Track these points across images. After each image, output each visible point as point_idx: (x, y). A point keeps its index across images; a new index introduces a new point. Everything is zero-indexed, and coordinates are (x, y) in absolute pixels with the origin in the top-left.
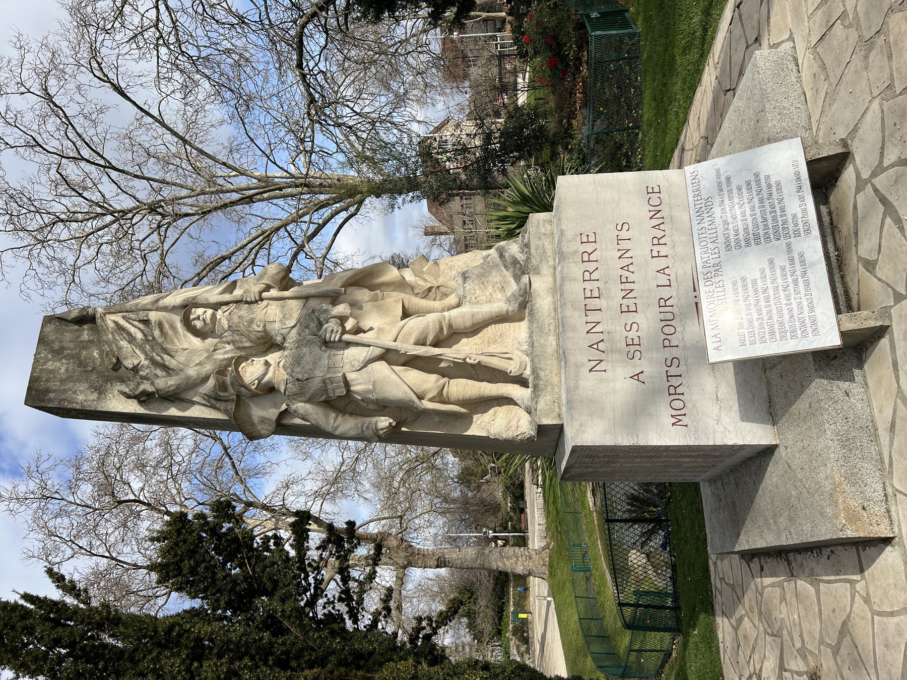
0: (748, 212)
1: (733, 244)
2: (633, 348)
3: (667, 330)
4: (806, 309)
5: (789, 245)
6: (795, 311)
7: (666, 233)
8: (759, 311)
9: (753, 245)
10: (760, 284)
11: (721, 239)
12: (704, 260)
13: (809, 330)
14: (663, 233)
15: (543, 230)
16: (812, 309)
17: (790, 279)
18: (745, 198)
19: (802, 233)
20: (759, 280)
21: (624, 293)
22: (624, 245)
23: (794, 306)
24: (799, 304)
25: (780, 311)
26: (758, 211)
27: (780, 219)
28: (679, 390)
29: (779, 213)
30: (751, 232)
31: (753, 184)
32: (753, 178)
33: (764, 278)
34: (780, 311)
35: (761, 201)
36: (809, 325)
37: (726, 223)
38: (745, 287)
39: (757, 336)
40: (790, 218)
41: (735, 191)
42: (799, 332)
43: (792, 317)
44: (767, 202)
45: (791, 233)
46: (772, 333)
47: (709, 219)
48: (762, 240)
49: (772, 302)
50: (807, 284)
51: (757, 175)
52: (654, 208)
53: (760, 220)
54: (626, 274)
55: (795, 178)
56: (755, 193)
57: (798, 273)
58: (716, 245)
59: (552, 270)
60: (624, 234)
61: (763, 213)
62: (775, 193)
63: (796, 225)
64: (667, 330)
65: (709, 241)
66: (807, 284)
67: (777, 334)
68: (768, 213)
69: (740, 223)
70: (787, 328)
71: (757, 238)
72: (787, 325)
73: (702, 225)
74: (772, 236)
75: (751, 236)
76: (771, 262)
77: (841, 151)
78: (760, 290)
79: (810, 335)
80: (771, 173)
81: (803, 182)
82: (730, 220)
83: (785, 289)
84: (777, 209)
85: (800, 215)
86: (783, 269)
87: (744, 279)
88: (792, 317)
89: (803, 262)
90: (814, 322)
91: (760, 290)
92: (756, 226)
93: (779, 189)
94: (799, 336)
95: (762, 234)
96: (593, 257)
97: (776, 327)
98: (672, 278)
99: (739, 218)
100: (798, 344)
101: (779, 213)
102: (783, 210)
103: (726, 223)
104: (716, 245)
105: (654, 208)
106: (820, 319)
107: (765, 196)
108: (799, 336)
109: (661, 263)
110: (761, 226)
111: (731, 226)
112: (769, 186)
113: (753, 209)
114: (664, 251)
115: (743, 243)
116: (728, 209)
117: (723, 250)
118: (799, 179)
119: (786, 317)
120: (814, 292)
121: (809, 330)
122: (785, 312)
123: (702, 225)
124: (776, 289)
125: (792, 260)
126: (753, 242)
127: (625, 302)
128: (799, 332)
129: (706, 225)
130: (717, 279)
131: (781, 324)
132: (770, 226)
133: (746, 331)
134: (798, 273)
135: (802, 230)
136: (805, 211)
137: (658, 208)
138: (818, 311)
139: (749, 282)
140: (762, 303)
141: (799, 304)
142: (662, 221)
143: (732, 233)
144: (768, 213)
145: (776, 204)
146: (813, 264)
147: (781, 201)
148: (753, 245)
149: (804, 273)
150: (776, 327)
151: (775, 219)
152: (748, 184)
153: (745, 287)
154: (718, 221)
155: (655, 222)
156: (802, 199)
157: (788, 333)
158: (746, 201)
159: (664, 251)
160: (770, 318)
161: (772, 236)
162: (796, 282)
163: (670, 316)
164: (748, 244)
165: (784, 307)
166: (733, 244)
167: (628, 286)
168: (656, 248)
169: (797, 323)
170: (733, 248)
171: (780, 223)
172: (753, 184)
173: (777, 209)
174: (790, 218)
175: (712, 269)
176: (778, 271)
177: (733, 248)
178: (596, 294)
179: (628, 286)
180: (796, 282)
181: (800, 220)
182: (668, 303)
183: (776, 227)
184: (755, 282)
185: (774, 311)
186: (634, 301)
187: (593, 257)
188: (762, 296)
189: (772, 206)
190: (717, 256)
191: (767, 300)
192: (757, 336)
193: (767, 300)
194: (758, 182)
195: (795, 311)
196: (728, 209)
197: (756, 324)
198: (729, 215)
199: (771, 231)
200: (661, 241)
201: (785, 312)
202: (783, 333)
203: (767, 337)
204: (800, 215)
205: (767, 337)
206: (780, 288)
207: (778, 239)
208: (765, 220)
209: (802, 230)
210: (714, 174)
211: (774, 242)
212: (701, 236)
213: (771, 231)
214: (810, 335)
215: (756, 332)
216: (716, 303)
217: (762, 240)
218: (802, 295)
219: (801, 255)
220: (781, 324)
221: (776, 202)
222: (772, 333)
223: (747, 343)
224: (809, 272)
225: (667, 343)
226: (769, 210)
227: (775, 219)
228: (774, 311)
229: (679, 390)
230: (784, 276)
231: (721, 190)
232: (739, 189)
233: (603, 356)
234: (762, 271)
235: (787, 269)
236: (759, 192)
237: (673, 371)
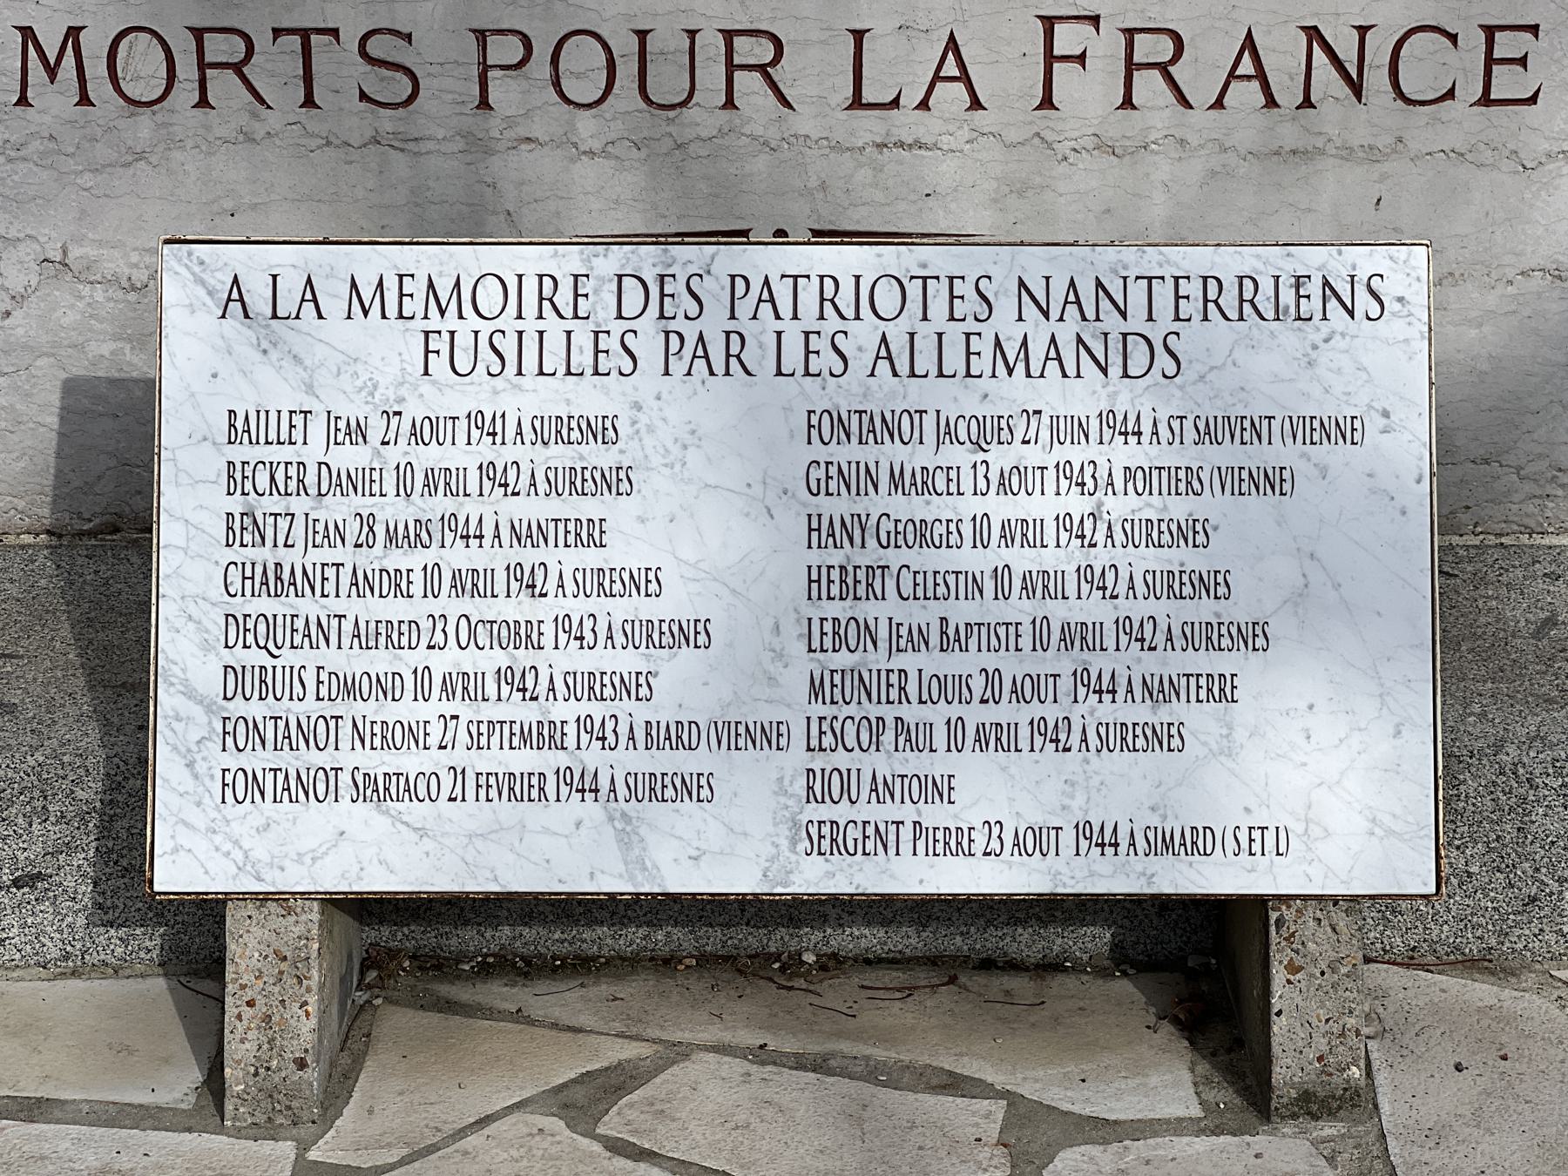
0: (1022, 560)
1: (846, 453)
5: (769, 736)
7: (1201, 118)
8: (415, 536)
9: (815, 557)
11: (887, 393)
12: (782, 292)
13: (258, 760)
14: (1202, 91)
16: (371, 789)
17: (565, 711)
18: (1121, 556)
19: (825, 812)
20: (591, 558)
23: (407, 710)
24: (414, 735)
25: (390, 635)
26: (1020, 609)
27: (938, 714)
29: (975, 715)
30: (894, 558)
31: (1203, 610)
32: (1238, 611)
33: (602, 582)
34: (390, 635)
35: (1078, 636)
36: (285, 759)
37: (988, 432)
38: (575, 482)
39: (272, 503)
40: (937, 764)
41: (1180, 508)
42: (256, 710)
43: (350, 689)
44: (1064, 664)
45: (841, 759)
46: (276, 581)
47: (1038, 350)
48: (835, 609)
49: (453, 606)
50: (519, 788)
51: (1252, 636)
52: (1379, 49)
53: (962, 612)
55: (1173, 825)
56: (1139, 609)
57: (593, 757)
58: (860, 363)
61: (1003, 636)
62: (1108, 711)
63: (882, 789)
65: (897, 333)
66: (519, 788)
67: (266, 605)
68: (990, 661)
69: (970, 506)
70: (288, 657)
72: (306, 658)
73: (1006, 307)
74: (843, 659)
75: (871, 555)
76: (689, 634)
77: (1279, 1074)
78: (529, 556)
79: (232, 761)
80: (1244, 710)
81: (1138, 863)
82: (1000, 458)
83: (517, 683)
84: (1004, 712)
85: (935, 815)
86: (635, 687)
87: (615, 482)
88: (350, 689)
89: (653, 788)
90: (301, 787)
91: (529, 556)
92: (928, 587)
93: (1124, 738)
94: (238, 707)
95: (869, 610)
97: (309, 607)
99: (1001, 508)
100: (190, 694)
101: (975, 715)
102: (994, 738)
103: (988, 432)
104: (860, 363)
105: (1379, 49)
106: (313, 823)
107: (1100, 663)
108: (238, 707)
109: (1007, 71)
110: (924, 614)
111: (959, 456)
112: (1160, 691)
113: (1040, 585)
114: (1087, 93)
115: (839, 506)
116: (1077, 454)
117: (820, 395)
118: (1164, 844)
120: (472, 814)
121: (258, 760)
122: (380, 662)
123: (1006, 307)
124: (523, 635)
125: (677, 736)
126: (835, 557)
128: (256, 710)
129: (1004, 323)
130: (648, 344)
132: (908, 661)
133: (313, 452)
134: (593, 757)
135: (842, 812)
136: (956, 843)
137: (1376, 80)
139: (588, 508)
140: (458, 557)
141: (414, 735)
142: (1288, 96)
143: (919, 457)
144: (990, 661)
145: (1036, 710)
146: (627, 837)
147: (1053, 736)
148: (815, 557)
149: (587, 787)
150: (309, 607)
151: (946, 688)
152: (1211, 585)
153: (575, 482)
154: (1013, 393)
155: (1284, 57)
156: (1036, 841)
157: (257, 657)
158: (1101, 558)
159: (1087, 93)
160: (362, 584)
161: (843, 659)
162: (548, 736)
164: (818, 531)
165: (420, 657)
166: (846, 453)
168: (1105, 48)
169: (310, 707)
170: (819, 452)
171: (912, 713)
172: (1203, 610)
173: (1004, 712)
174: (937, 764)
175: (714, 324)
176: (626, 661)
177: (819, 452)
180: (548, 736)
181: (907, 813)
183: (896, 686)
184: (590, 534)
185: (394, 609)
188: (491, 558)
189: (1027, 689)
190: (793, 357)
191: (468, 584)
192: (272, 503)
193: (468, 584)
194: (1208, 637)
195: (371, 710)
196: (1077, 454)
197: (338, 509)
198: (1032, 456)
199: (878, 659)
201: (380, 662)
202: (269, 634)
203: (265, 554)
204: (935, 815)
205: (265, 554)
206: (524, 657)
207: (816, 690)
208: (952, 639)
209: (842, 812)
210: (1328, 409)
211: (799, 669)
212: (939, 291)
213: (878, 659)
214: (232, 761)
215: (299, 505)
216: (508, 322)
217: (835, 609)
218: (460, 756)
219: (692, 788)
221: (1052, 713)
222: (276, 581)
223: (239, 453)
224: (590, 810)
226: (1011, 666)
227: (946, 688)
228: (394, 609)
230: (591, 686)
231: (1207, 433)
232: (1190, 533)
234: (644, 582)
235: (625, 706)
236: (1135, 633)
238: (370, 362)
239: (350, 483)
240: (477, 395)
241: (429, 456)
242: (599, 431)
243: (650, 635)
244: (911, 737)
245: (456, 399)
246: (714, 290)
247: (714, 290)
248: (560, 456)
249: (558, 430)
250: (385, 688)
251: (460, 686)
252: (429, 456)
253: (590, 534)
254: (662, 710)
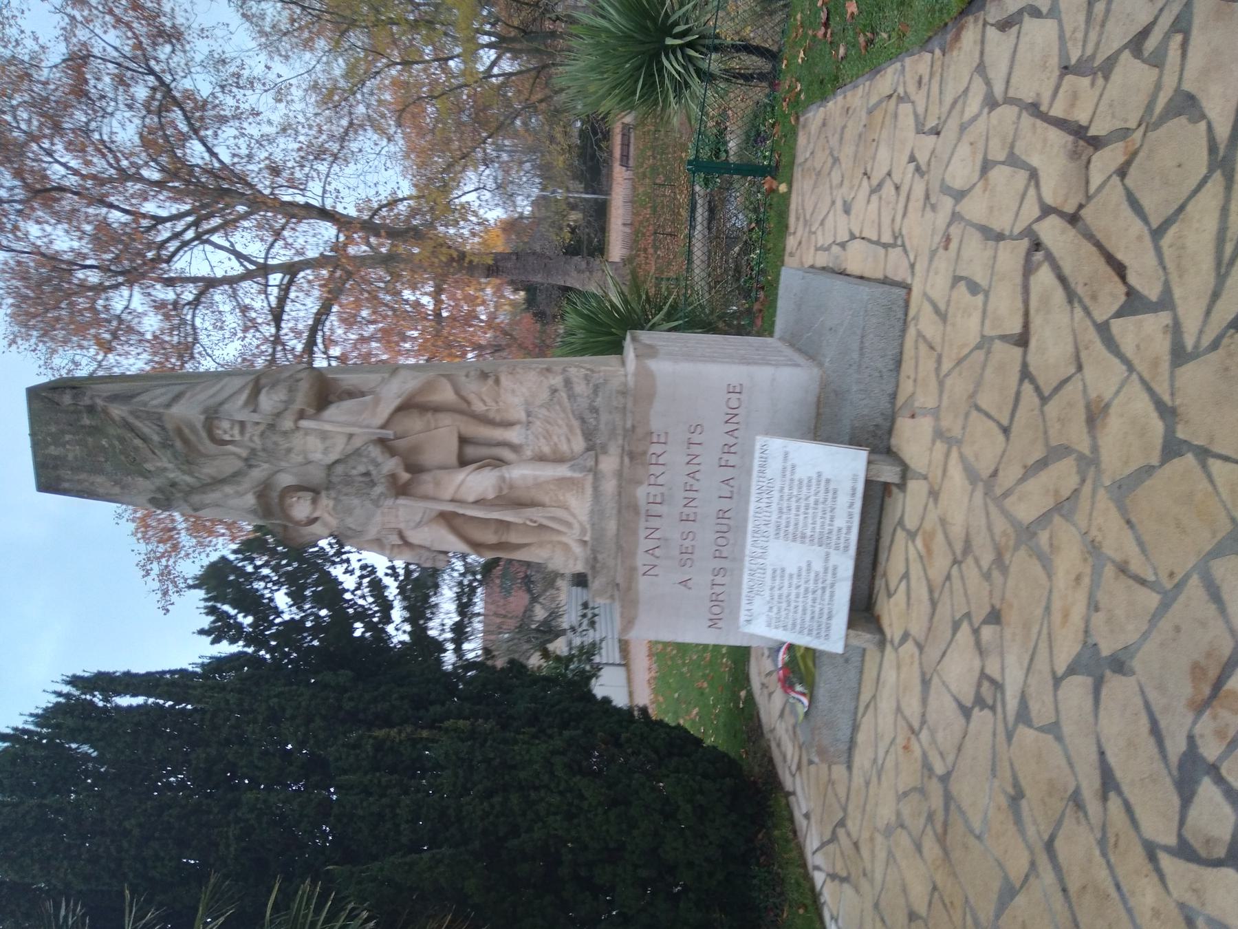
2: (686, 556)
3: (721, 541)
4: (825, 616)
5: (828, 555)
6: (817, 615)
10: (795, 581)
13: (823, 634)
15: (615, 404)
16: (830, 618)
21: (686, 501)
22: (695, 449)
27: (827, 528)
28: (720, 597)
29: (828, 522)
33: (799, 576)
34: (804, 610)
38: (782, 576)
44: (820, 506)
46: (794, 625)
54: (691, 481)
59: (619, 450)
60: (696, 438)
63: (839, 538)
64: (721, 541)
69: (792, 516)
71: (803, 537)
83: (814, 592)
87: (783, 570)
89: (834, 574)
90: (828, 628)
96: (661, 460)
98: (735, 490)
102: (832, 519)
109: (729, 473)
110: (810, 526)
115: (790, 536)
117: (772, 536)
119: (808, 617)
121: (823, 634)
124: (806, 590)
125: (826, 570)
127: (686, 510)
130: (761, 561)
131: (803, 621)
132: (818, 530)
138: (834, 622)
140: (793, 597)
149: (832, 585)
150: (799, 621)
162: (824, 589)
163: (724, 528)
164: (794, 540)
167: (691, 494)
168: (726, 457)
174: (835, 530)
178: (658, 500)
179: (691, 494)
180: (824, 589)
182: (727, 515)
185: (800, 609)
186: (694, 510)
187: (661, 460)
188: (794, 592)
193: (797, 596)
195: (817, 615)
197: (783, 613)
200: (733, 450)
202: (802, 628)
204: (844, 531)
205: (790, 626)
211: (816, 547)
219: (835, 568)
220: (803, 621)
225: (717, 554)
227: (823, 525)
229: (720, 597)
233: (656, 562)
234: (800, 570)
237: (719, 580)
238: (759, 605)
239: (779, 610)
240: (767, 588)
241: (776, 597)
242: (774, 571)
243: (809, 570)
244: (830, 532)
245: (767, 593)
246: (754, 549)
247: (754, 549)
248: (778, 578)
249: (774, 578)
250: (813, 612)
251: (814, 600)
252: (776, 597)
253: (791, 576)
254: (822, 570)
